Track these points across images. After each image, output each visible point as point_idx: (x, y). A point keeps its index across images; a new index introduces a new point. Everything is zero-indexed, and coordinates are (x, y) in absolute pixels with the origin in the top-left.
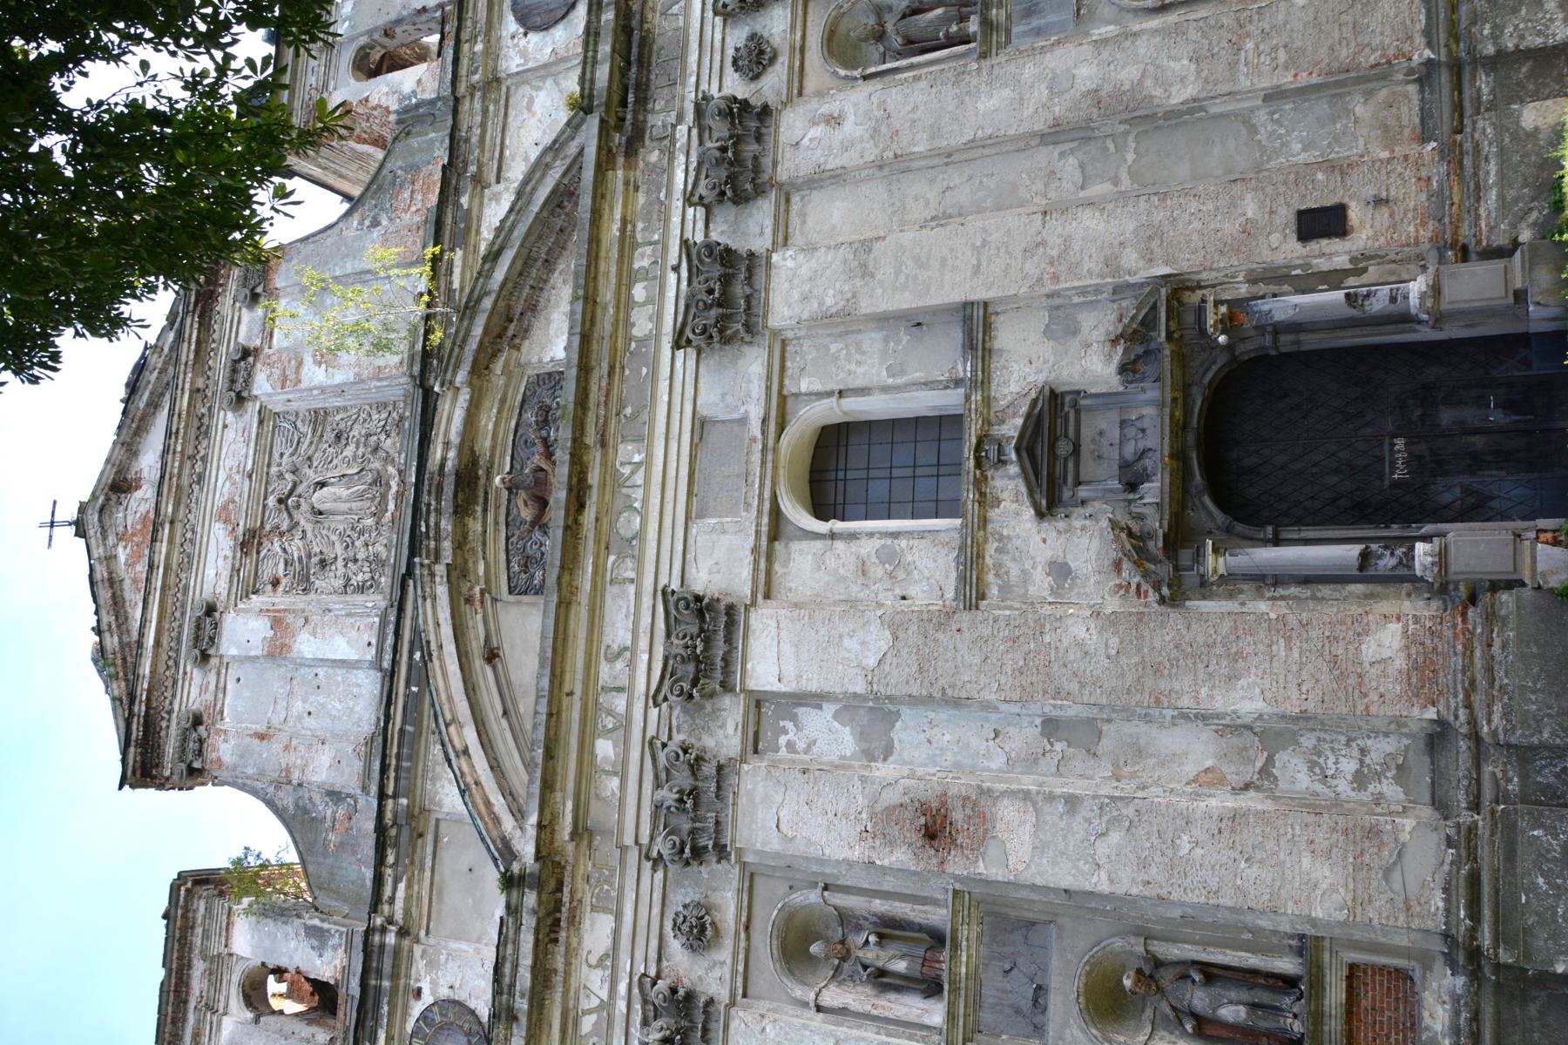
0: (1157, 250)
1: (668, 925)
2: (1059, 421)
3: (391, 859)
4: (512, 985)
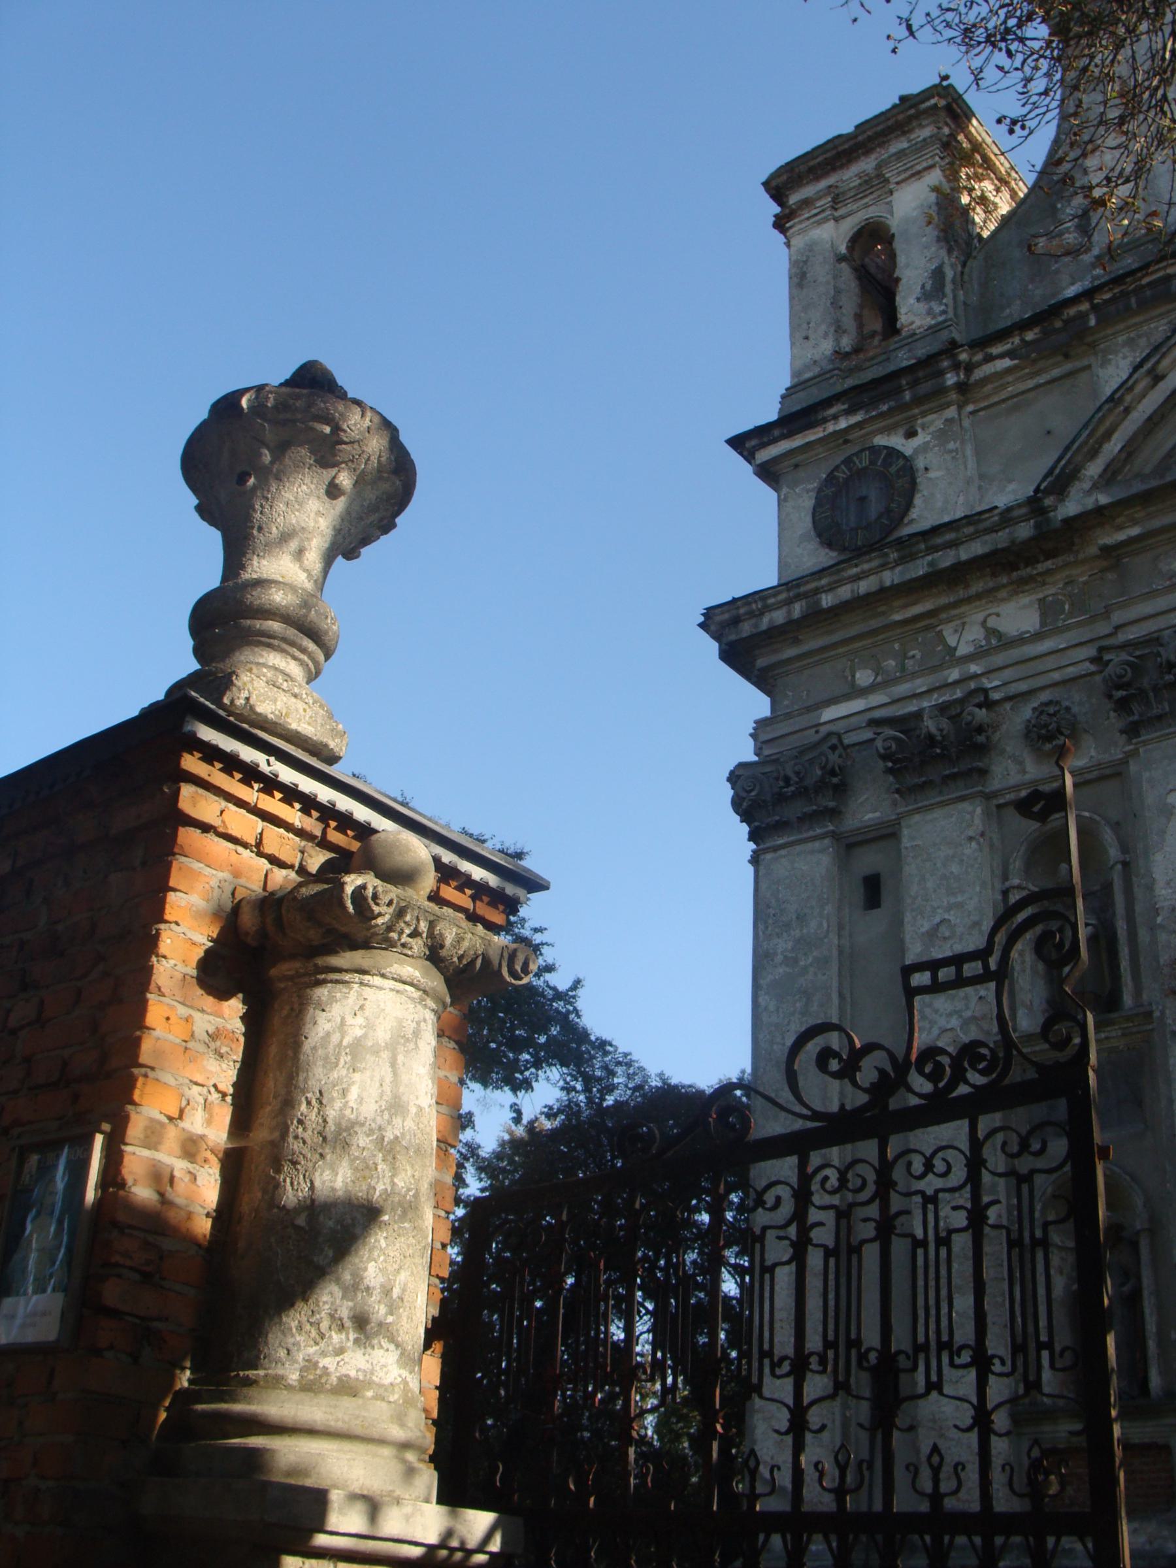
1: (1044, 697)
3: (1030, 336)
4: (936, 549)
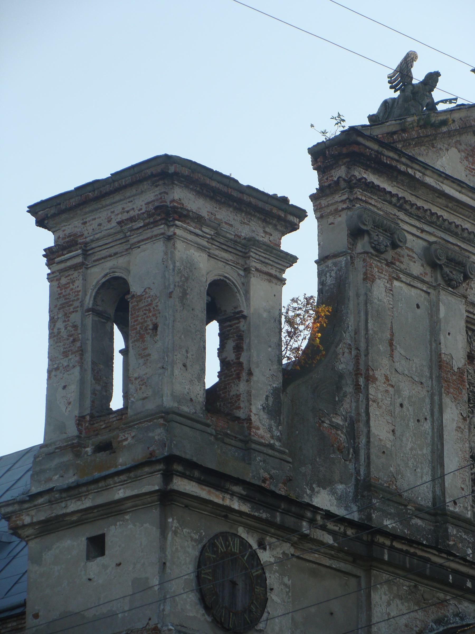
3: (350, 532)
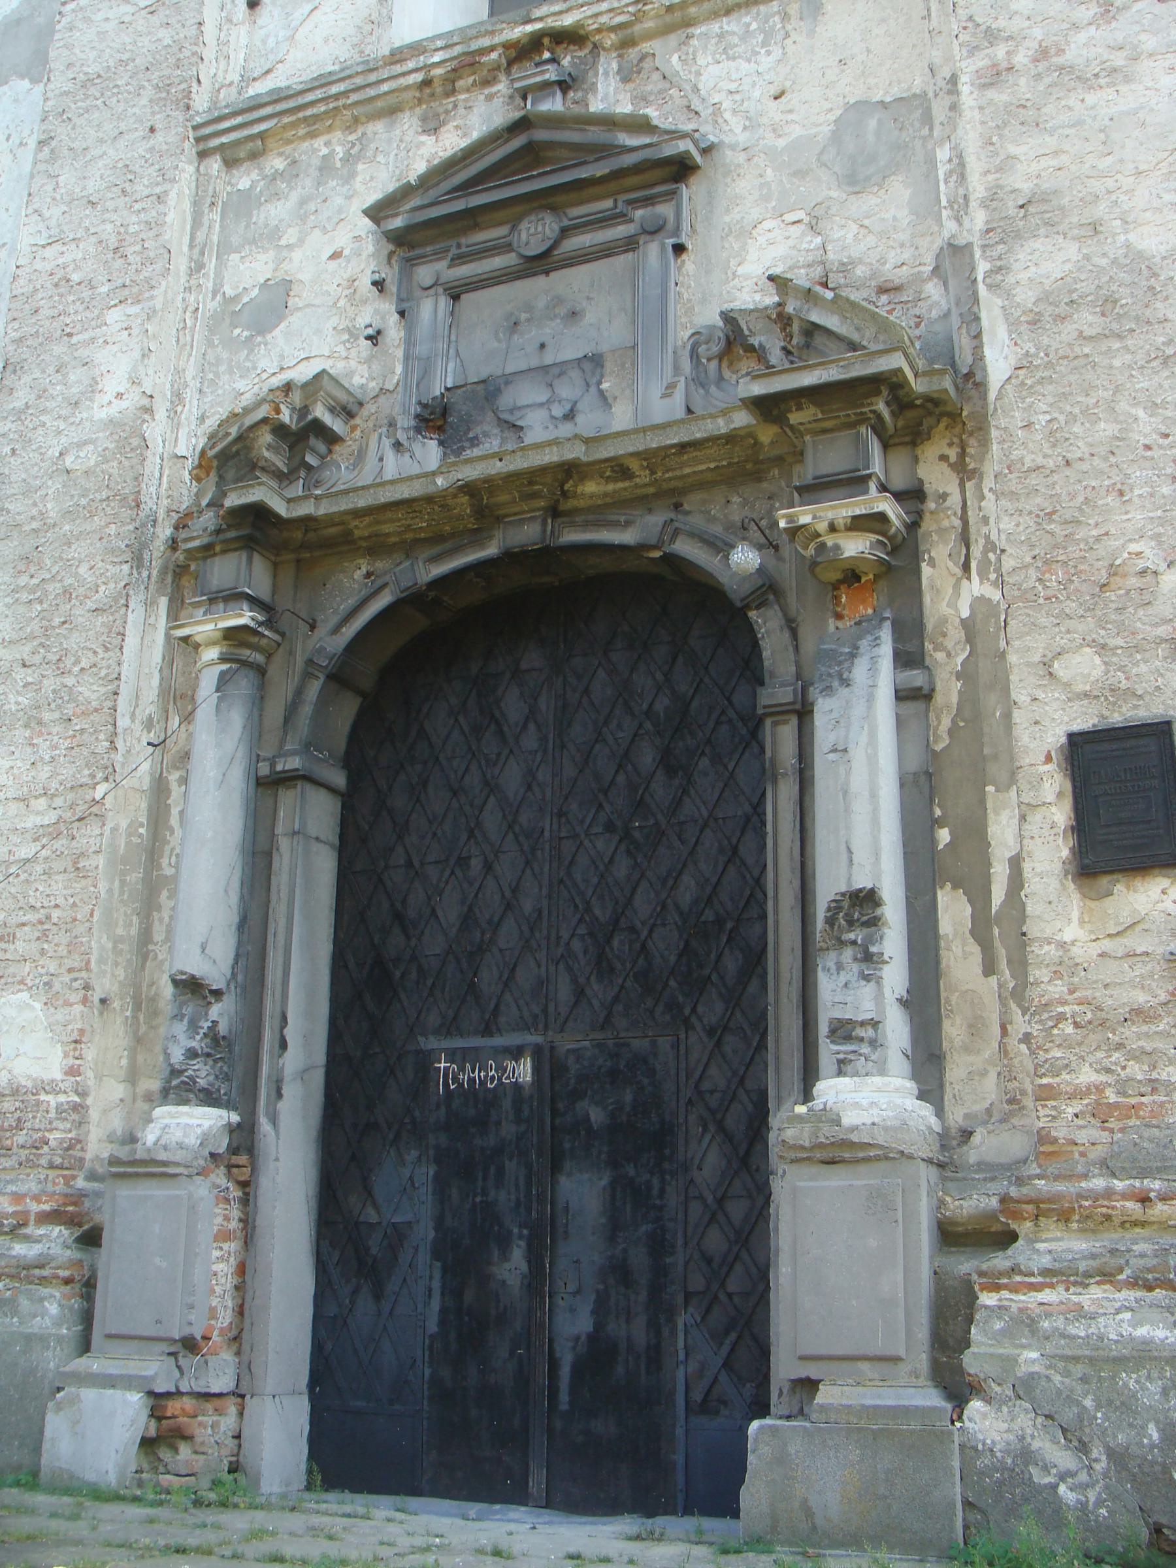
0: (1068, 331)
2: (608, 203)
